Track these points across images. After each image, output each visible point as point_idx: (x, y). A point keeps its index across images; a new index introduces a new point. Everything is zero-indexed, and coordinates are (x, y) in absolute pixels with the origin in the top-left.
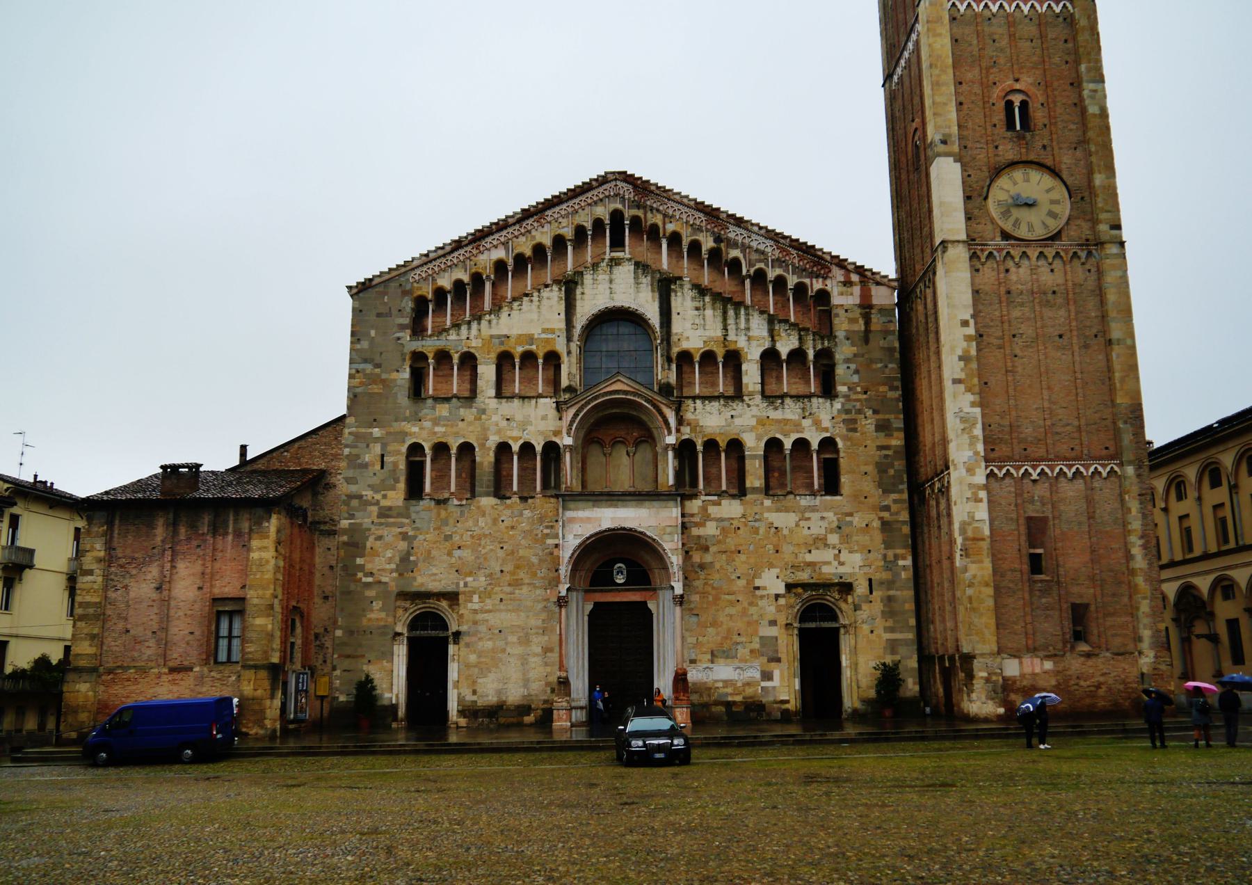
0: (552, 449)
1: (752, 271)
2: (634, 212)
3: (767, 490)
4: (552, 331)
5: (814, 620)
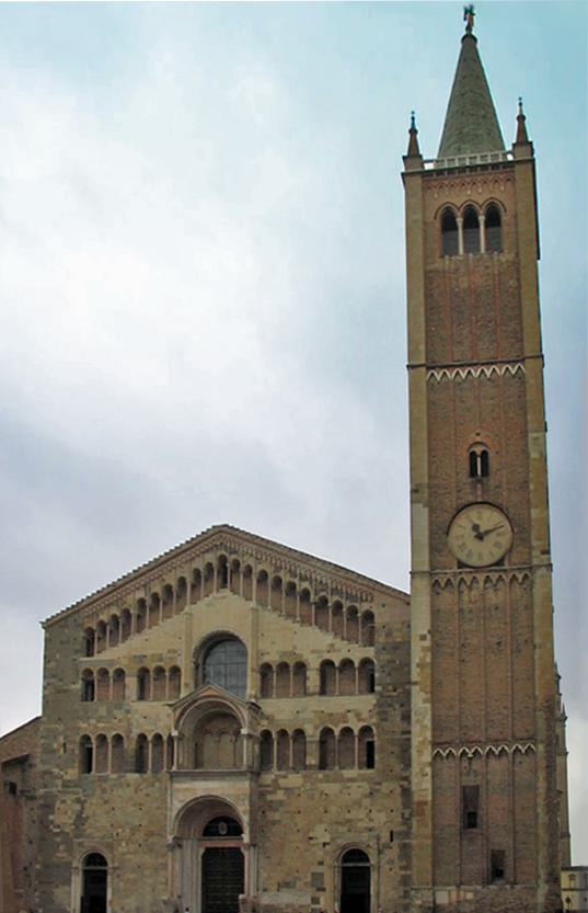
0: (171, 739)
1: (317, 597)
2: (233, 556)
3: (323, 765)
4: (175, 651)
5: (353, 861)
